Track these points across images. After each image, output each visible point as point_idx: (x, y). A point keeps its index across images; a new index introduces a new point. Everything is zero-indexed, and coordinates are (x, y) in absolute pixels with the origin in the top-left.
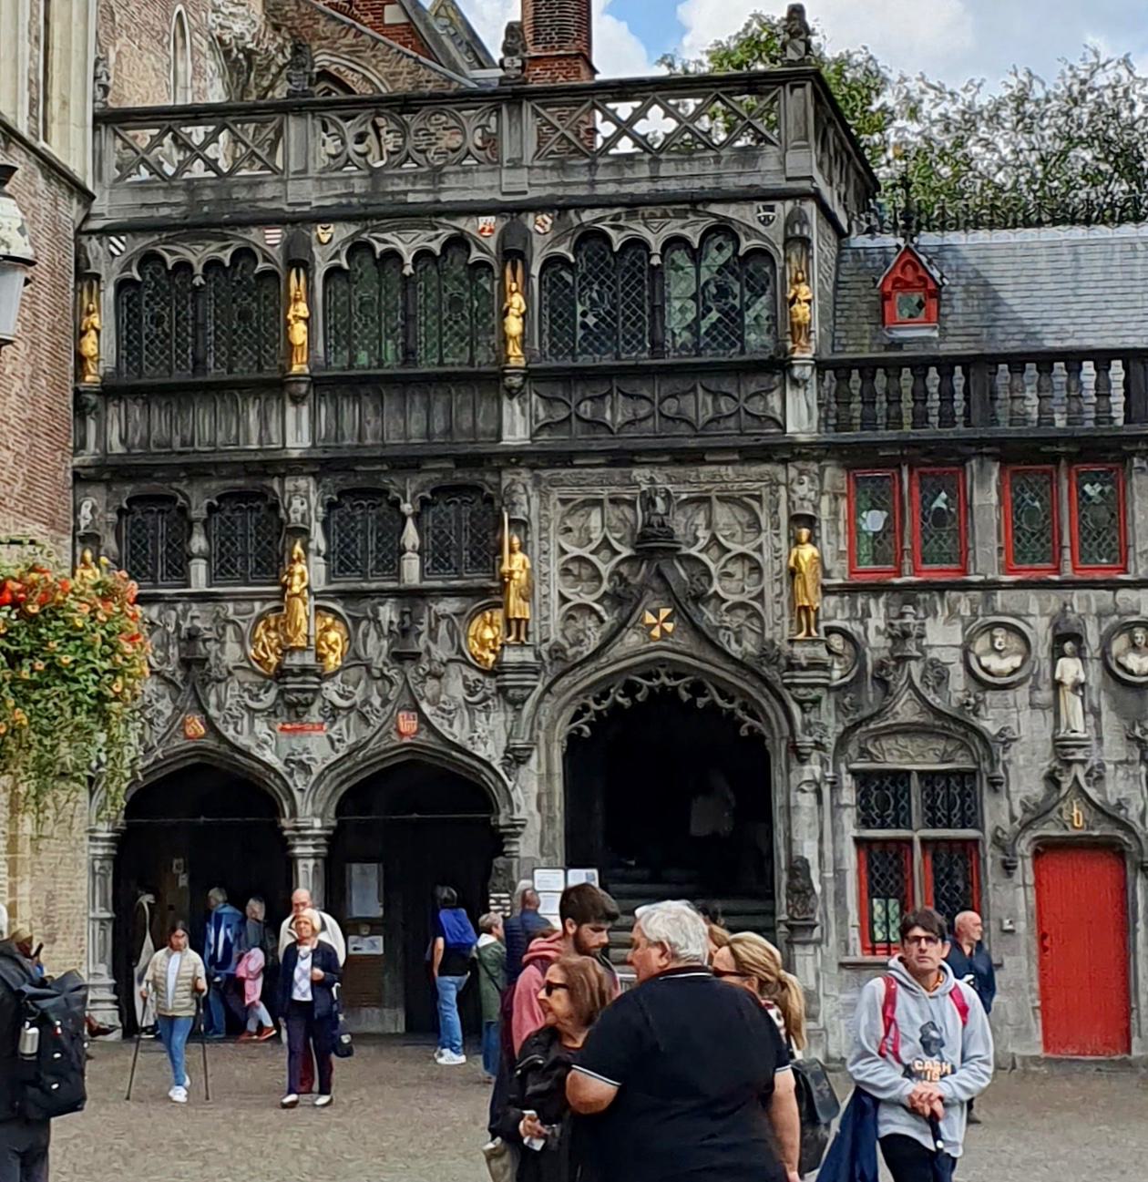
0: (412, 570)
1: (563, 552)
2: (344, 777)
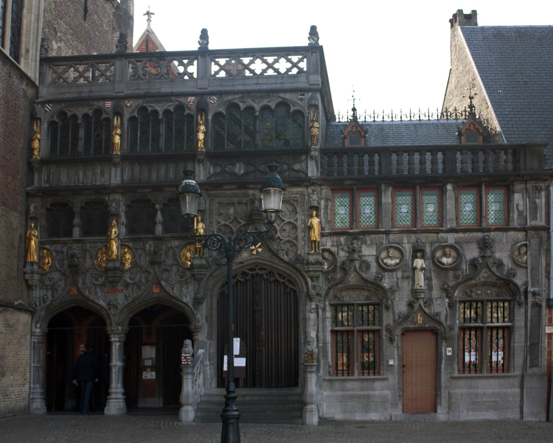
0: (159, 229)
1: (219, 223)
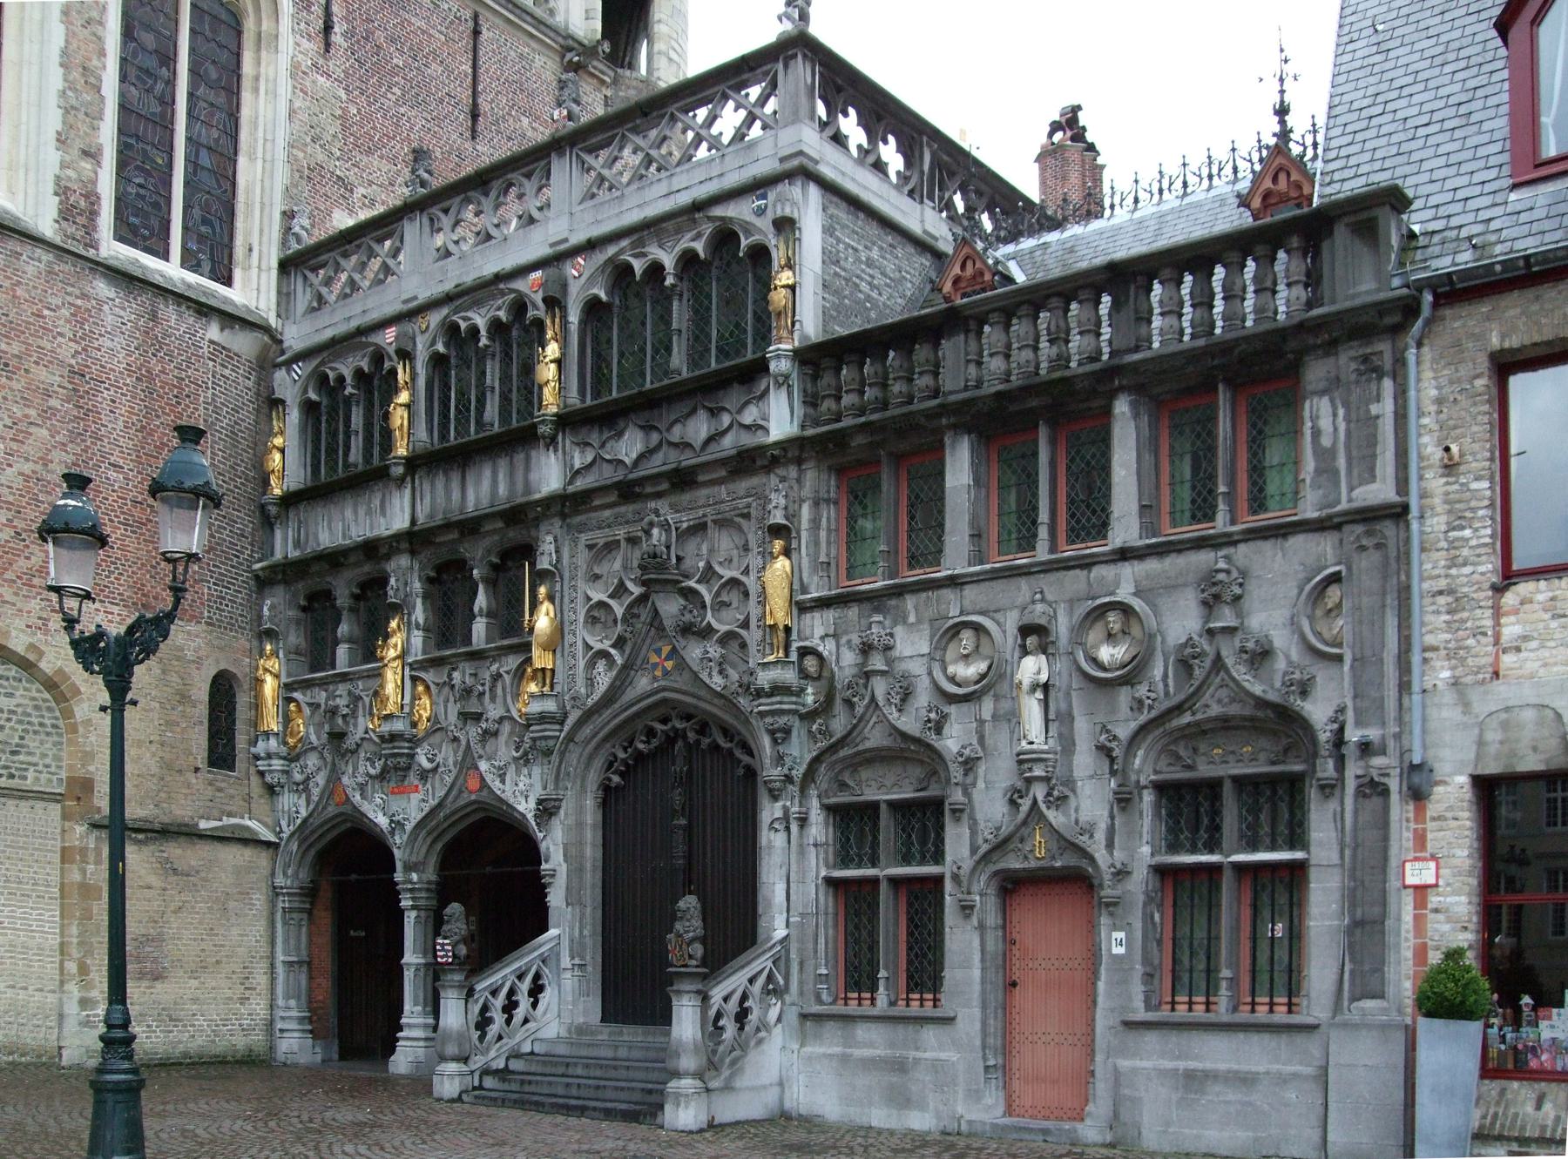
0: (479, 628)
1: (589, 599)
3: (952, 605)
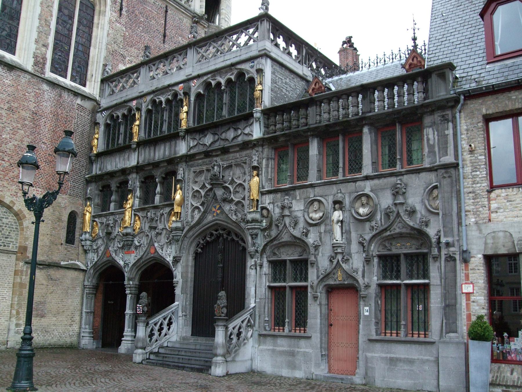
1: (193, 189)
2: (139, 268)
3: (311, 193)
